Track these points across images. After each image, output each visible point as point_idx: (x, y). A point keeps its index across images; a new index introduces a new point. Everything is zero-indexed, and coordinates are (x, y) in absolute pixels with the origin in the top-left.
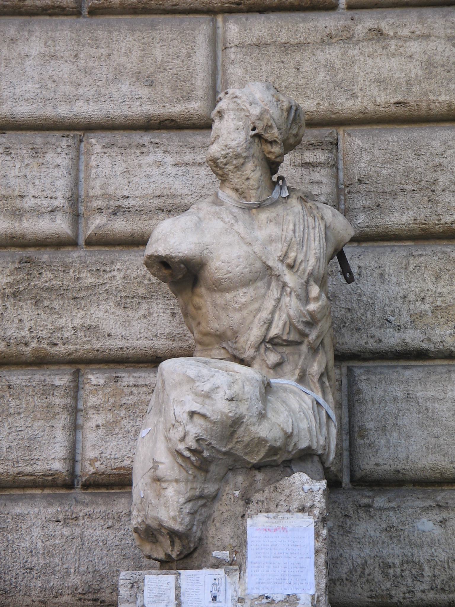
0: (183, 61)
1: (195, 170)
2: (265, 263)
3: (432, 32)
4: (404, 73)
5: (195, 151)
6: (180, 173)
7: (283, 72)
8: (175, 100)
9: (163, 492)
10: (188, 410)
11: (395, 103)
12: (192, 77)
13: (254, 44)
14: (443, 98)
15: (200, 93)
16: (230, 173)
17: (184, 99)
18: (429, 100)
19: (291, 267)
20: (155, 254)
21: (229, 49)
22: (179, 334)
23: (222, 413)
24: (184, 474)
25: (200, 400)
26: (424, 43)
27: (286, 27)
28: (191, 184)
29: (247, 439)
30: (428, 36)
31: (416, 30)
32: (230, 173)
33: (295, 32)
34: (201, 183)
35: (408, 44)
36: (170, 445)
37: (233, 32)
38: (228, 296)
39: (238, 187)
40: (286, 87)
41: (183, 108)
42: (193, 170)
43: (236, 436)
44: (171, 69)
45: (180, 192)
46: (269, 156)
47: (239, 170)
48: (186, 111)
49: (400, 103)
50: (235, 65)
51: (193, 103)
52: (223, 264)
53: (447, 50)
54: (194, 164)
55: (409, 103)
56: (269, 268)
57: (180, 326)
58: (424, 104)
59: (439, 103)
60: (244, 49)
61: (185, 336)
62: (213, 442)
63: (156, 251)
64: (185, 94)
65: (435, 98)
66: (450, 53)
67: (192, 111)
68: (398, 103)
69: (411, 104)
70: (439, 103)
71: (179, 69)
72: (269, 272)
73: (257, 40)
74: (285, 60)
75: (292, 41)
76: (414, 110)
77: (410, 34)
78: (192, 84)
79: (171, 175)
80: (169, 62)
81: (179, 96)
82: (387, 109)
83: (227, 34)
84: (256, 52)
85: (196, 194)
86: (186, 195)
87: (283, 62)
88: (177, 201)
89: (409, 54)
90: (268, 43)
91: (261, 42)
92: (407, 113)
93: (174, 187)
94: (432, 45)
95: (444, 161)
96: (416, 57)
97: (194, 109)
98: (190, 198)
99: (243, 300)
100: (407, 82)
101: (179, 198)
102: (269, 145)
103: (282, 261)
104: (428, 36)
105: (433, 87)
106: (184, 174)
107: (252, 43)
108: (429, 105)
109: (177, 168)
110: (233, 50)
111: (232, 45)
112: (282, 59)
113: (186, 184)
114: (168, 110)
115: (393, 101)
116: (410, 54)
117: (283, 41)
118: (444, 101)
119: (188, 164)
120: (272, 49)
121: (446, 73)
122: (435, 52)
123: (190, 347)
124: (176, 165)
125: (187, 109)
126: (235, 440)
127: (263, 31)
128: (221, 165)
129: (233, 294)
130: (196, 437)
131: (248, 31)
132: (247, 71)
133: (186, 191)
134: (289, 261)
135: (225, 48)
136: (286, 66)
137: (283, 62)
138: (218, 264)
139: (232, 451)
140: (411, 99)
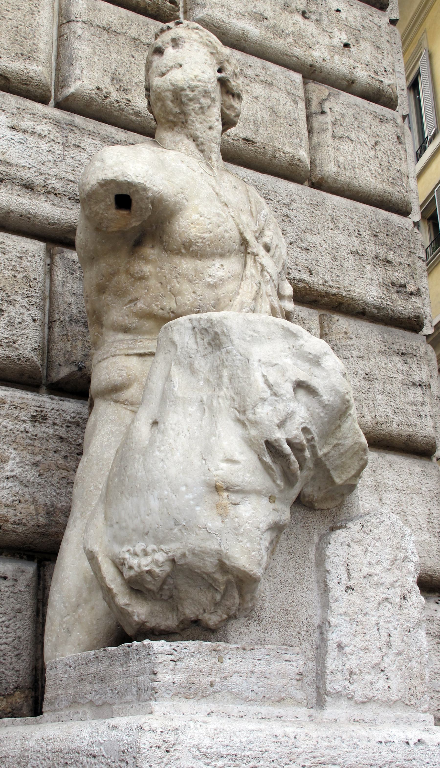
0: (25, 16)
1: (34, 141)
2: (241, 234)
3: (274, 82)
4: (250, 112)
5: (35, 119)
6: (16, 138)
7: (134, 67)
8: (13, 54)
9: (232, 510)
10: (294, 379)
11: (244, 139)
12: (35, 36)
13: (103, 27)
14: (287, 149)
15: (42, 56)
16: (193, 114)
17: (24, 57)
18: (275, 146)
19: (267, 249)
20: (121, 179)
21: (75, 23)
22: (6, 338)
23: (337, 393)
24: (269, 483)
25: (306, 366)
26: (267, 91)
27: (137, 23)
28: (29, 156)
29: (349, 442)
30: (271, 84)
31: (260, 74)
32: (193, 114)
33: (146, 32)
34: (42, 158)
35: (253, 85)
36: (253, 432)
37: (80, 7)
38: (199, 264)
39: (198, 133)
40: (136, 83)
41: (22, 67)
42: (31, 139)
43: (339, 435)
44: (10, 19)
45: (15, 161)
46: (228, 112)
47: (203, 113)
48: (25, 71)
49: (247, 140)
50: (83, 42)
51: (35, 65)
52: (202, 219)
53: (288, 104)
54: (33, 133)
55: (256, 143)
56: (244, 242)
57: (9, 329)
58: (270, 149)
59: (284, 153)
60: (92, 29)
61: (14, 343)
62: (316, 438)
63: (123, 175)
64: (25, 52)
65: (280, 147)
66: (291, 108)
67: (32, 74)
68: (246, 140)
69: (258, 144)
70: (284, 153)
71: (20, 23)
72: (242, 248)
73: (107, 24)
74: (136, 56)
75: (142, 39)
76: (260, 153)
77: (255, 77)
78: (34, 44)
79: (5, 138)
80: (9, 11)
81: (19, 52)
82: (235, 142)
83: (72, 8)
84: (106, 36)
85: (35, 169)
86: (24, 167)
87: (133, 57)
88: (12, 171)
89: (255, 95)
90: (118, 31)
91: (110, 28)
92: (252, 154)
93: (8, 153)
94: (275, 95)
95: (292, 214)
96: (261, 100)
97: (35, 72)
98: (28, 171)
99: (221, 273)
100: (254, 122)
101: (15, 168)
102: (231, 97)
103: (257, 238)
104: (271, 84)
105: (278, 135)
106: (22, 141)
107: (101, 25)
108: (274, 151)
109: (14, 132)
110: (79, 24)
111: (79, 19)
112: (133, 53)
113: (23, 153)
114: (4, 64)
115: (242, 136)
116: (256, 96)
117: (133, 36)
118: (289, 153)
119: (25, 131)
120: (122, 39)
121: (288, 126)
122: (278, 102)
123: (19, 359)
124: (13, 128)
125: (27, 69)
126: (335, 442)
127: (113, 18)
128: (184, 100)
129: (208, 262)
130: (302, 423)
131: (97, 11)
132: (95, 53)
133: (23, 162)
134: (266, 239)
135: (68, 22)
136: (136, 62)
137: (133, 57)
138: (195, 216)
139: (323, 459)
140: (259, 139)
